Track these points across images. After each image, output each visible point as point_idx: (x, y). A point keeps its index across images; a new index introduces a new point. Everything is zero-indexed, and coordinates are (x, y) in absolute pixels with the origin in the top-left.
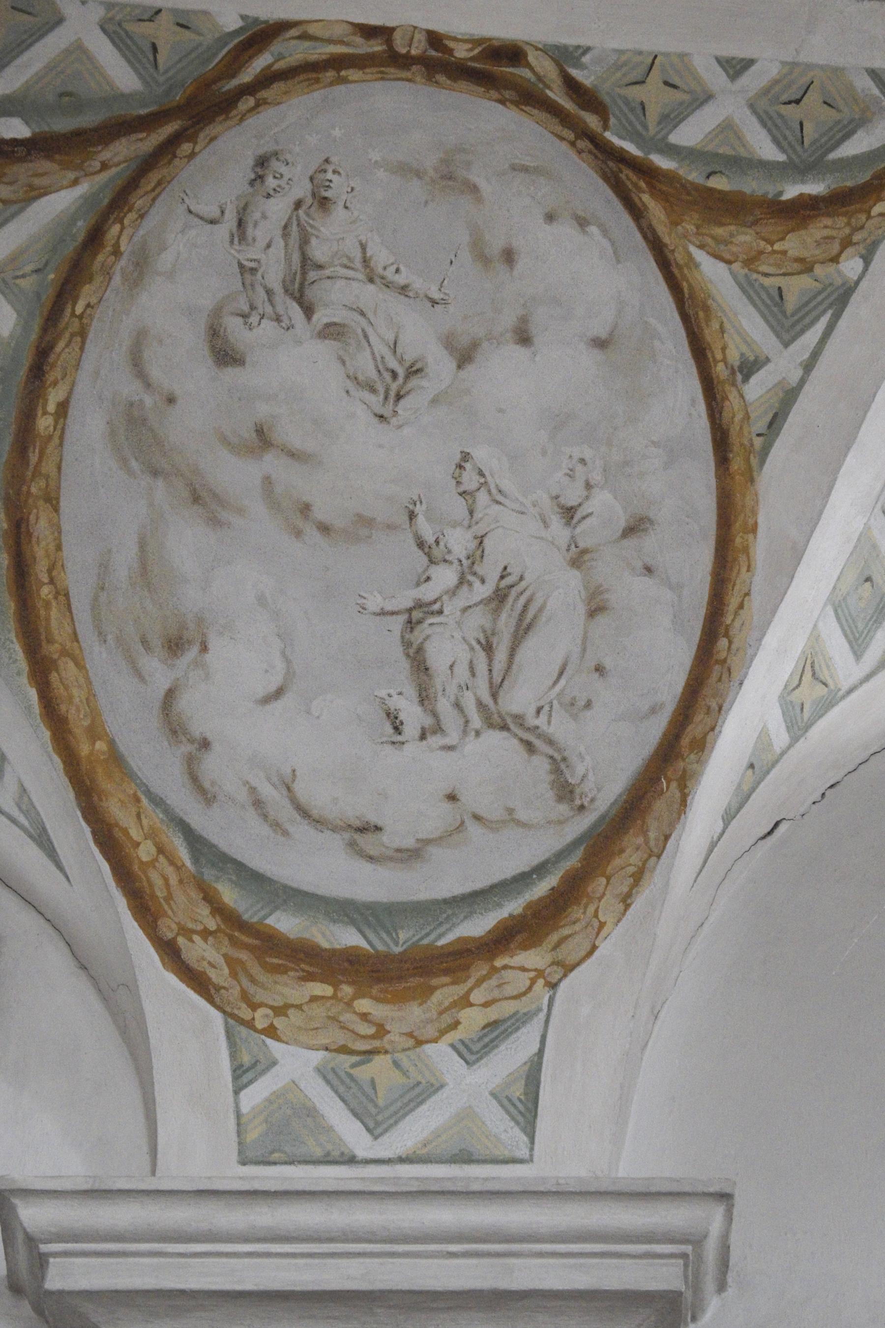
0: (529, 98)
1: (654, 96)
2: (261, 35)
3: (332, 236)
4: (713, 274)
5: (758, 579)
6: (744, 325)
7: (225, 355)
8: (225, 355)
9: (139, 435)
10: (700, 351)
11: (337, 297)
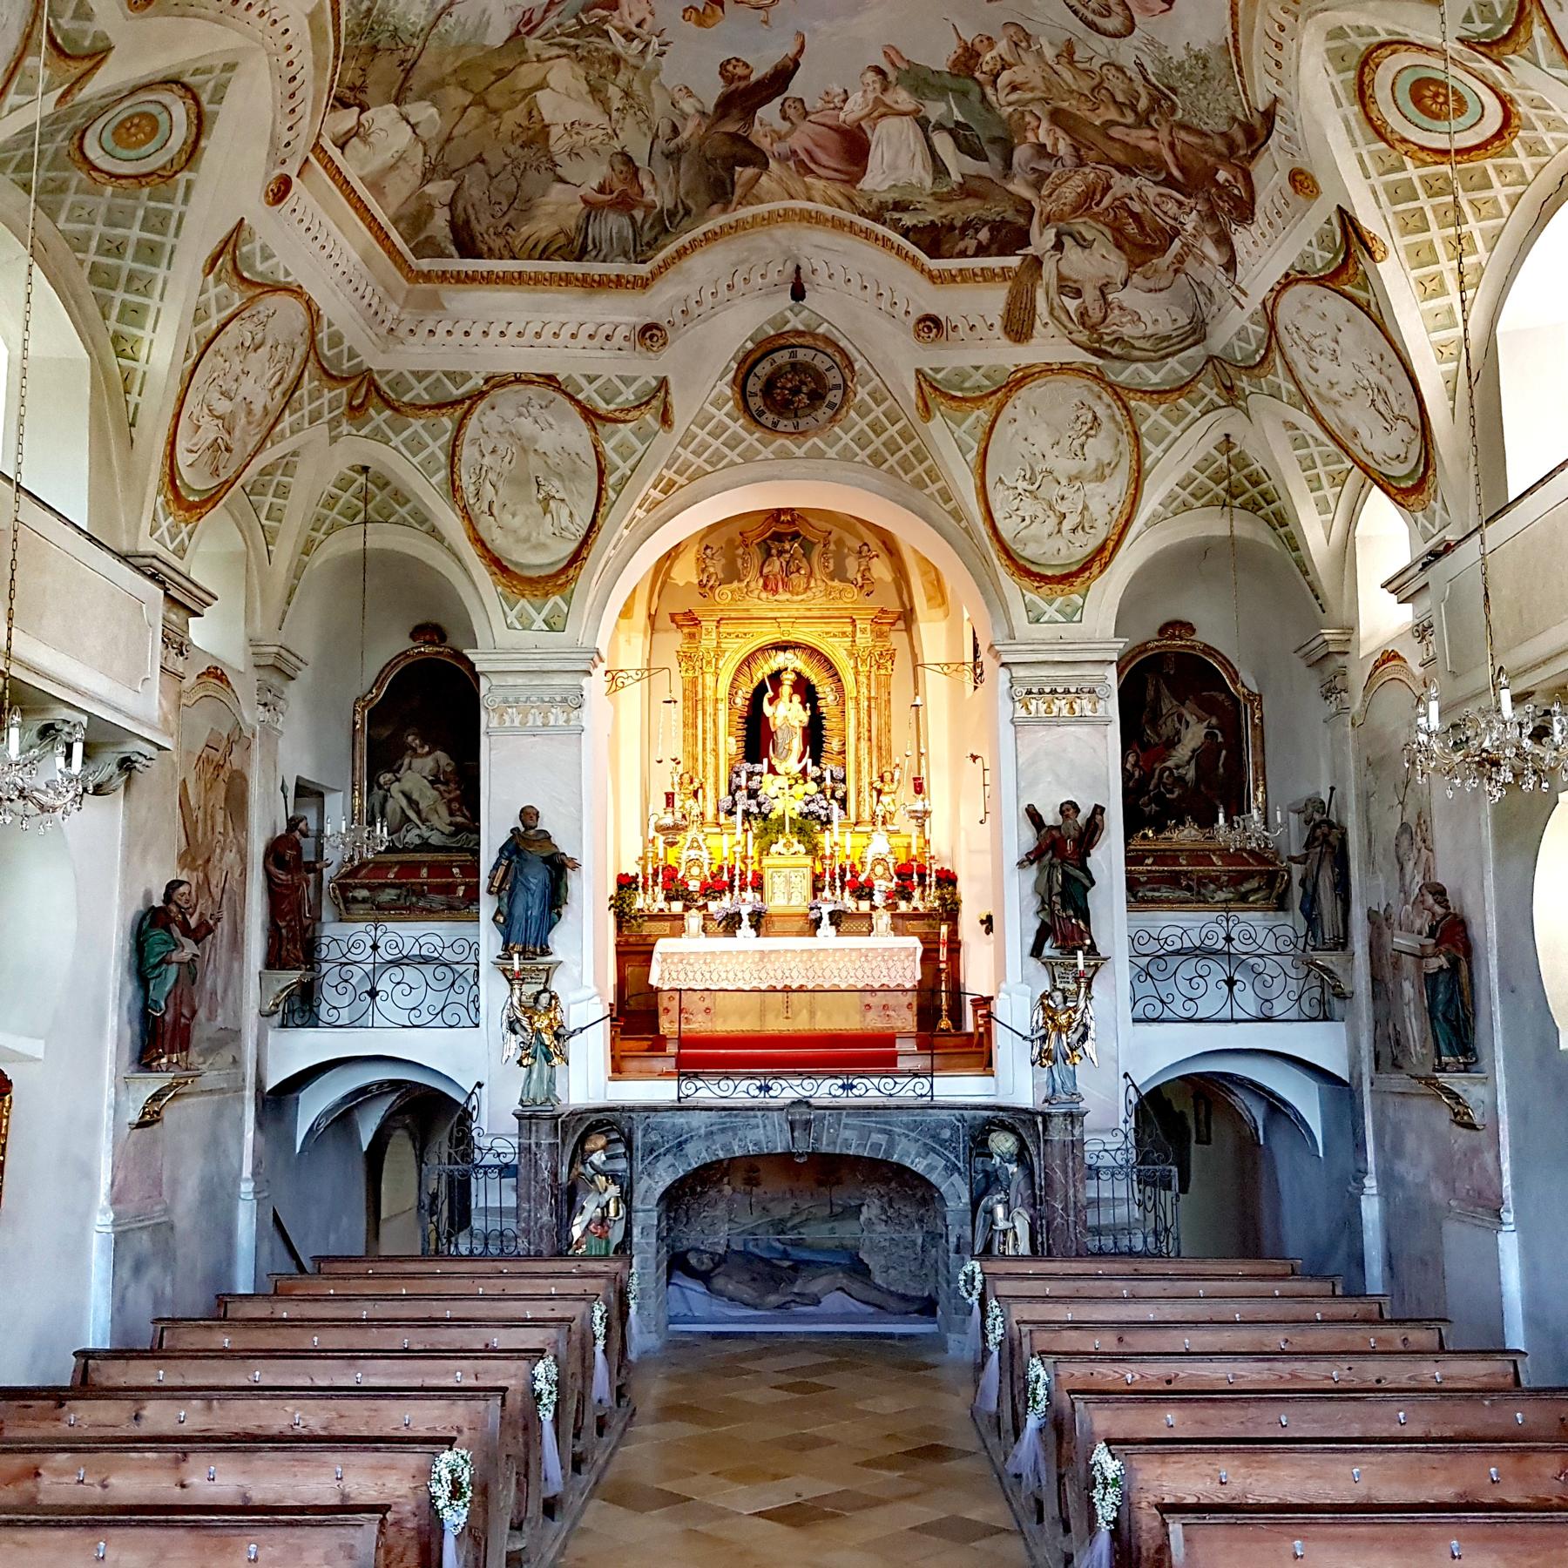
0: (1297, 281)
1: (1308, 262)
2: (1264, 304)
3: (1305, 332)
4: (1347, 288)
5: (1404, 354)
6: (1361, 295)
7: (1316, 371)
8: (1316, 371)
9: (1318, 394)
10: (1361, 308)
11: (1315, 343)
